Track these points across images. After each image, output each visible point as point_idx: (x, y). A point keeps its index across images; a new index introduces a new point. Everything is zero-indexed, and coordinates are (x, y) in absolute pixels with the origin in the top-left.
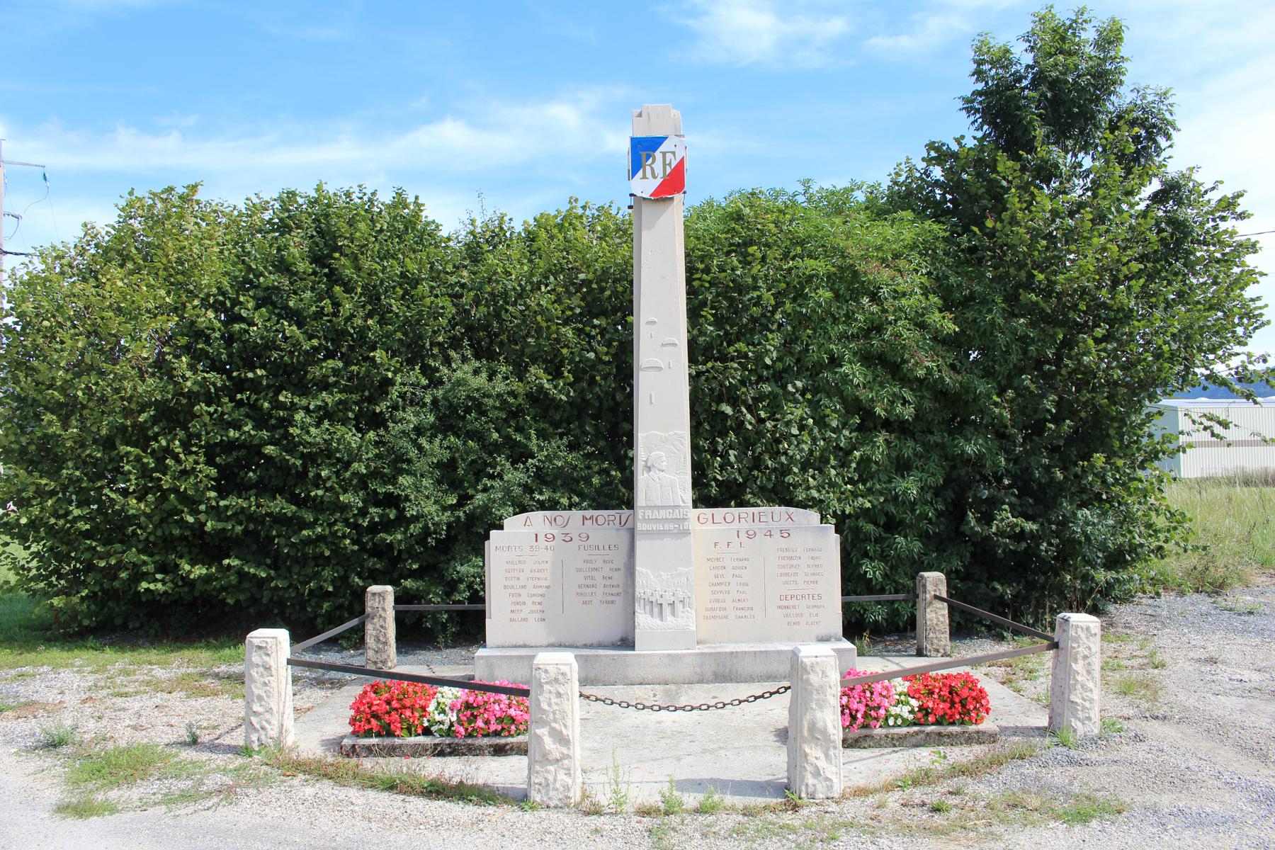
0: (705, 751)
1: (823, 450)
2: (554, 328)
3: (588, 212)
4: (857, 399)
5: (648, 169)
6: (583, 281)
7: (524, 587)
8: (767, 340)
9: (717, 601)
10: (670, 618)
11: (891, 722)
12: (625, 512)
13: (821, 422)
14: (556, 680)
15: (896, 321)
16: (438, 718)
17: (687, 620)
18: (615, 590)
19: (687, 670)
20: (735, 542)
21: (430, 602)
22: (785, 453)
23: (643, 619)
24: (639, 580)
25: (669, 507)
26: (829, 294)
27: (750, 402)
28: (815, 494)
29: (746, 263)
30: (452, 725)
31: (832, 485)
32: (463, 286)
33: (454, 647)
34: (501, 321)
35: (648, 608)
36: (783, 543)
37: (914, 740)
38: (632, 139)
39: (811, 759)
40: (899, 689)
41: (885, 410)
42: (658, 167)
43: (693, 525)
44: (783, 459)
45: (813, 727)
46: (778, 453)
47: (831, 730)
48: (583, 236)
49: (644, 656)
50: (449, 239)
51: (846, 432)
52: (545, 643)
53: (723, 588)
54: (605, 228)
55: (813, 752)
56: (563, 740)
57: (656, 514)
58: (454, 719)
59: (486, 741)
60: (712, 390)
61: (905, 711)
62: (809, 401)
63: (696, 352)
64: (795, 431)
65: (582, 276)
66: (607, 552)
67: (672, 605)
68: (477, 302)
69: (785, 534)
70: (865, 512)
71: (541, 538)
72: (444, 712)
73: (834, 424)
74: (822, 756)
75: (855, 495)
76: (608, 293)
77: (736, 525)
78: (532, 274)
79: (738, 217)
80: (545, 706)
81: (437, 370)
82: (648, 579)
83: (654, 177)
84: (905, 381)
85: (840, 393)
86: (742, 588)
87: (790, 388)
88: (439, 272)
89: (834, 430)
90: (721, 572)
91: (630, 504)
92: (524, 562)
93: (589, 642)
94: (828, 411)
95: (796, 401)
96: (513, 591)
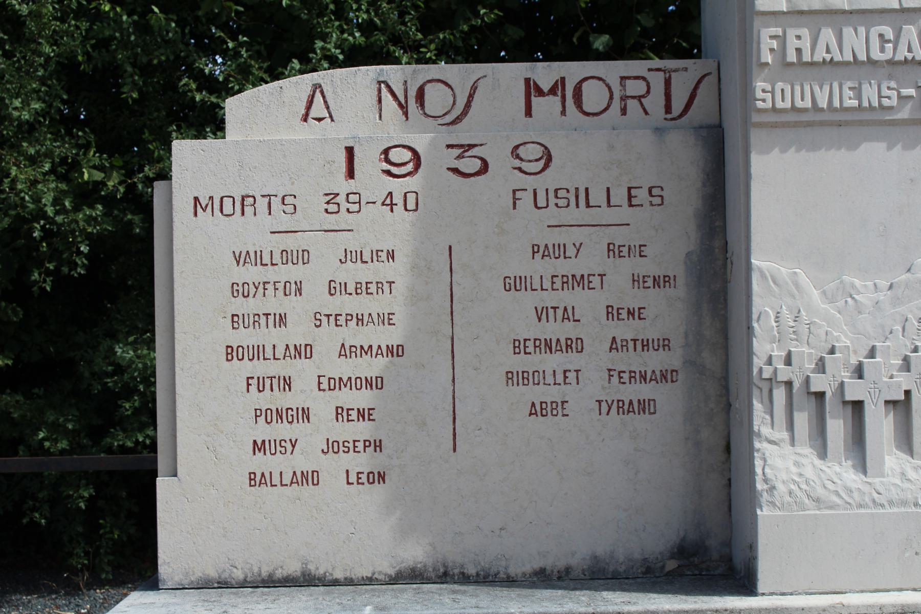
7: (303, 351)
18: (655, 361)
21: (39, 450)
23: (784, 463)
25: (883, 13)
35: (802, 420)
52: (387, 568)
66: (624, 213)
71: (369, 164)
92: (304, 257)
93: (554, 560)
96: (260, 368)
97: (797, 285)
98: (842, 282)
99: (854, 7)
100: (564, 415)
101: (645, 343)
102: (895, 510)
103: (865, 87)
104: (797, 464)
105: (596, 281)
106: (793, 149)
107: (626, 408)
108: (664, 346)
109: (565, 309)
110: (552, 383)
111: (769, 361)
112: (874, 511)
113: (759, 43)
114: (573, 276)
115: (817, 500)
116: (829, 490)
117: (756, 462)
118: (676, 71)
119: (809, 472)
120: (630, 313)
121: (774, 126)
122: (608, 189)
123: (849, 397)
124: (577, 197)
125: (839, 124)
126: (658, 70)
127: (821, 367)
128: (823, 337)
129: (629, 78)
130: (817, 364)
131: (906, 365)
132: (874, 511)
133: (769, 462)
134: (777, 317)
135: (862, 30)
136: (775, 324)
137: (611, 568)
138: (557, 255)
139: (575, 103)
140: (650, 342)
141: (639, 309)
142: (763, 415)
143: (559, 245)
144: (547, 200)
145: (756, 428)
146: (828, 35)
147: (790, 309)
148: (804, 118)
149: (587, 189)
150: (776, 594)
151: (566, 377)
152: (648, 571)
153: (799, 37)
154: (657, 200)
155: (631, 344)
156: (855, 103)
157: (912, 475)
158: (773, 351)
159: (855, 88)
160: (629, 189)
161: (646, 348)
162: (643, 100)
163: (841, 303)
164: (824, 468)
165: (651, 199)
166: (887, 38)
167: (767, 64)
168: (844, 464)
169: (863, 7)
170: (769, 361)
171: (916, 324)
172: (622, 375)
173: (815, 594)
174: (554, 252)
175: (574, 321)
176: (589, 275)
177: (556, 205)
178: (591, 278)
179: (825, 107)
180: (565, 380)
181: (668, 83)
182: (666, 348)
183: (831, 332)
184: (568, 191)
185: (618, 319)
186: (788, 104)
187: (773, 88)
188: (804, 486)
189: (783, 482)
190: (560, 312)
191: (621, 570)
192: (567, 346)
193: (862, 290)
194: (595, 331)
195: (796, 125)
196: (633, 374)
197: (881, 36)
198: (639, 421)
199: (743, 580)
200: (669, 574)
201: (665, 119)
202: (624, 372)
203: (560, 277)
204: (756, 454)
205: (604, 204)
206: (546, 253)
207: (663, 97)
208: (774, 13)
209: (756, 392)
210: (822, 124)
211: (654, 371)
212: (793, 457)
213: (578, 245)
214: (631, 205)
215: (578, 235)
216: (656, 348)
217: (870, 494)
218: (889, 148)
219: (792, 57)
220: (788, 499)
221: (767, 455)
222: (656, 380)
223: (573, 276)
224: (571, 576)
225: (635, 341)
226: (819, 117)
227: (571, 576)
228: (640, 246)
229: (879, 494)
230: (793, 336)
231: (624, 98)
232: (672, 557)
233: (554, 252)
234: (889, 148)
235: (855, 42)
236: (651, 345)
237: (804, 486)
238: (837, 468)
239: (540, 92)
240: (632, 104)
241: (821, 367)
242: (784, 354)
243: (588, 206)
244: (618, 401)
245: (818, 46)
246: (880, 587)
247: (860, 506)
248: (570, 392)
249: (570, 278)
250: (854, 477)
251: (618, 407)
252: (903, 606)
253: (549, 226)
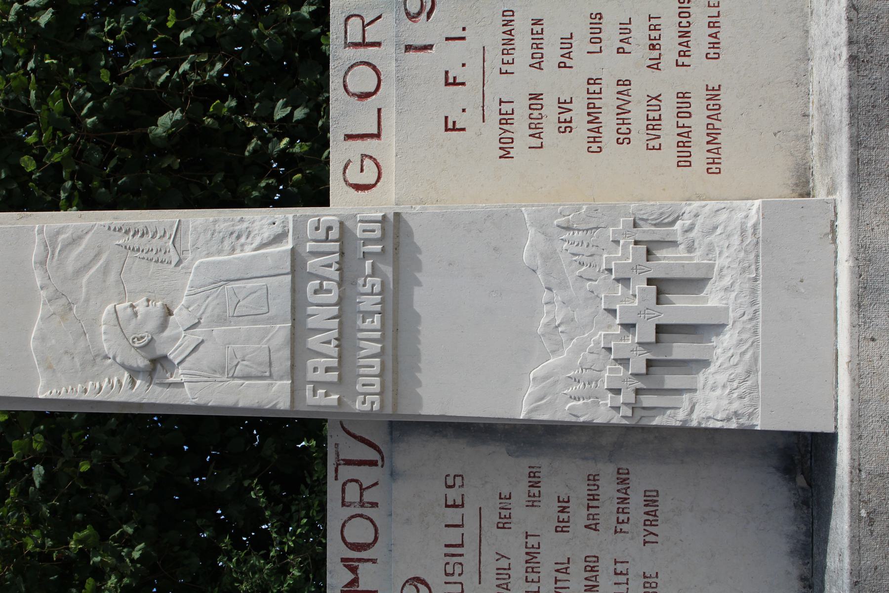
9: (653, 125)
10: (713, 299)
12: (339, 446)
17: (722, 225)
18: (608, 489)
20: (447, 57)
23: (712, 400)
24: (562, 411)
25: (296, 290)
35: (672, 381)
49: (859, 402)
53: (609, 102)
57: (322, 341)
66: (470, 512)
67: (662, 287)
77: (386, 57)
86: (611, 35)
90: (551, 110)
91: (313, 426)
97: (545, 378)
98: (543, 335)
99: (289, 317)
100: (657, 576)
101: (591, 497)
102: (760, 299)
103: (362, 307)
104: (713, 389)
105: (532, 541)
106: (418, 374)
107: (651, 518)
108: (594, 480)
109: (557, 571)
110: (626, 586)
111: (617, 409)
112: (760, 320)
113: (320, 406)
114: (527, 562)
115: (749, 373)
116: (740, 361)
117: (711, 426)
118: (338, 454)
119: (722, 378)
120: (563, 510)
121: (396, 392)
122: (446, 526)
123: (652, 338)
124: (453, 555)
125: (396, 330)
126: (336, 470)
127: (624, 362)
128: (594, 356)
129: (343, 498)
130: (620, 364)
131: (625, 281)
132: (760, 320)
133: (711, 414)
134: (575, 399)
135: (310, 309)
136: (581, 402)
137: (803, 538)
138: (507, 577)
139: (365, 550)
140: (590, 493)
141: (559, 501)
142: (666, 416)
143: (498, 574)
144: (455, 583)
145: (678, 424)
146: (314, 342)
147: (567, 387)
148: (389, 365)
149: (446, 546)
150: (836, 415)
151: (621, 573)
152: (806, 503)
153: (315, 369)
154: (458, 481)
155: (592, 511)
156: (377, 317)
157: (727, 281)
158: (607, 404)
159: (363, 317)
160: (447, 506)
161: (596, 497)
162: (364, 487)
163: (564, 337)
164: (718, 364)
165: (457, 486)
166: (318, 287)
167: (339, 399)
168: (714, 344)
169: (289, 309)
170: (617, 409)
171: (584, 268)
172: (620, 521)
173: (837, 378)
174: (504, 579)
175: (568, 563)
176: (526, 547)
177: (460, 575)
178: (529, 545)
179: (380, 345)
180: (624, 574)
181: (348, 462)
182: (596, 478)
183: (590, 349)
184: (448, 563)
185: (568, 522)
186: (377, 380)
187: (362, 394)
188: (735, 384)
189: (730, 403)
190: (560, 576)
191: (805, 528)
192: (592, 571)
193: (552, 317)
194: (577, 544)
195: (395, 372)
196: (620, 510)
197: (316, 292)
198: (664, 507)
200: (810, 485)
201: (382, 466)
202: (618, 518)
203: (527, 574)
204: (703, 426)
205: (460, 530)
206: (505, 586)
207: (362, 467)
208: (293, 392)
209: (644, 422)
210: (395, 347)
211: (618, 491)
212: (707, 391)
213: (499, 557)
214: (463, 505)
215: (489, 557)
216: (596, 487)
217: (744, 322)
218: (419, 284)
219: (333, 376)
220: (746, 400)
221: (704, 415)
222: (626, 489)
223: (527, 562)
224: (809, 576)
225: (589, 507)
226: (389, 351)
227: (809, 576)
228: (500, 498)
229: (744, 314)
230: (593, 385)
231: (362, 504)
232: (793, 480)
233: (504, 579)
234: (419, 284)
235: (321, 315)
236: (593, 492)
237: (735, 384)
238: (719, 351)
239: (355, 582)
240: (368, 497)
241: (624, 362)
242: (610, 395)
243: (461, 546)
244: (645, 525)
245: (324, 352)
246: (833, 316)
247: (755, 333)
248: (635, 571)
249: (528, 565)
250: (727, 336)
251: (651, 525)
252: (852, 305)
253: (480, 583)
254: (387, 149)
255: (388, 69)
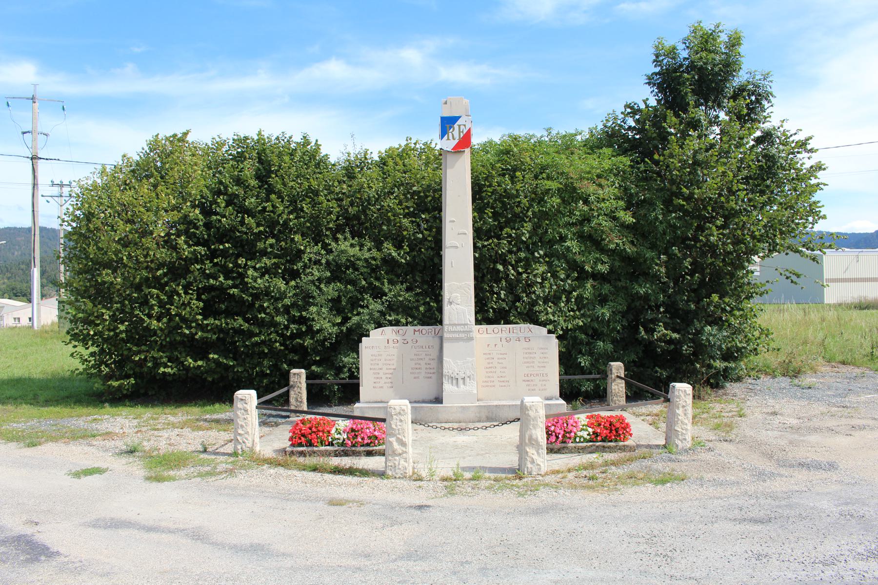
0: (478, 455)
1: (555, 291)
2: (398, 220)
3: (418, 146)
4: (575, 261)
5: (450, 134)
6: (414, 191)
8: (523, 227)
10: (462, 386)
11: (578, 440)
13: (555, 275)
14: (400, 413)
15: (598, 216)
16: (337, 436)
17: (471, 387)
18: (432, 371)
19: (471, 415)
20: (499, 344)
22: (534, 292)
23: (447, 387)
24: (445, 365)
26: (558, 201)
27: (513, 262)
28: (552, 318)
29: (513, 178)
30: (344, 440)
31: (561, 311)
32: (344, 194)
33: (339, 405)
34: (366, 215)
36: (526, 345)
37: (590, 450)
38: (442, 118)
39: (529, 454)
40: (583, 423)
41: (592, 267)
42: (456, 133)
43: (475, 334)
44: (533, 296)
45: (531, 438)
46: (530, 293)
47: (540, 440)
48: (414, 162)
50: (334, 165)
51: (569, 282)
54: (428, 158)
55: (531, 451)
56: (403, 444)
57: (454, 329)
58: (345, 437)
59: (362, 448)
60: (491, 256)
61: (584, 434)
62: (546, 262)
63: (479, 233)
64: (539, 280)
65: (415, 188)
67: (464, 379)
68: (352, 204)
69: (527, 339)
70: (580, 328)
72: (340, 433)
73: (562, 276)
74: (536, 453)
75: (574, 318)
76: (430, 198)
78: (384, 188)
79: (507, 152)
80: (394, 426)
81: (330, 245)
82: (450, 365)
83: (454, 139)
84: (603, 250)
85: (564, 256)
86: (503, 370)
87: (536, 254)
88: (330, 186)
89: (562, 280)
91: (441, 322)
93: (417, 400)
94: (558, 269)
95: (540, 262)
199: (442, 403)
235: (459, 328)
254: (485, 335)
255: (498, 335)
